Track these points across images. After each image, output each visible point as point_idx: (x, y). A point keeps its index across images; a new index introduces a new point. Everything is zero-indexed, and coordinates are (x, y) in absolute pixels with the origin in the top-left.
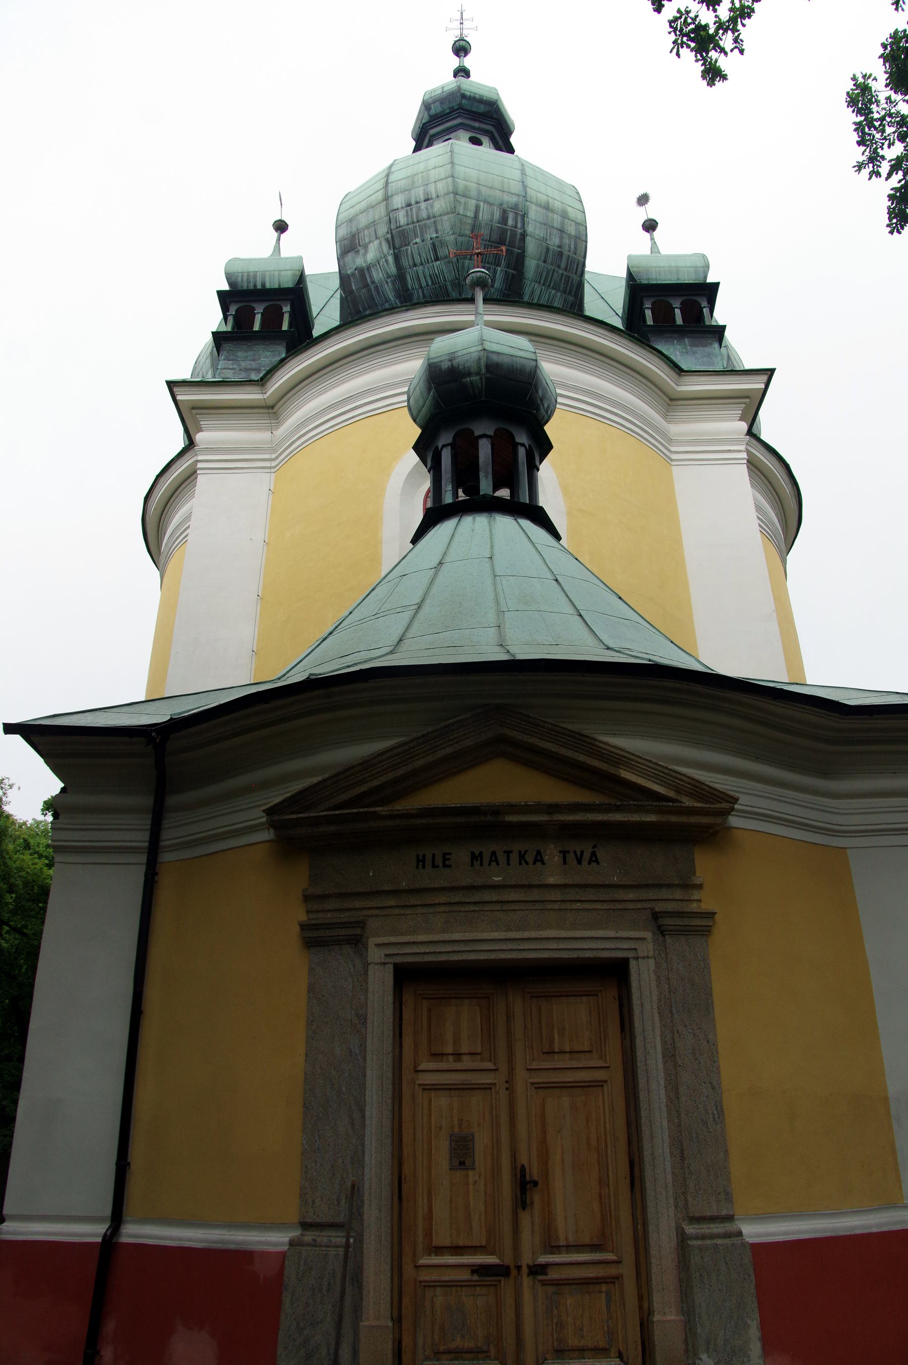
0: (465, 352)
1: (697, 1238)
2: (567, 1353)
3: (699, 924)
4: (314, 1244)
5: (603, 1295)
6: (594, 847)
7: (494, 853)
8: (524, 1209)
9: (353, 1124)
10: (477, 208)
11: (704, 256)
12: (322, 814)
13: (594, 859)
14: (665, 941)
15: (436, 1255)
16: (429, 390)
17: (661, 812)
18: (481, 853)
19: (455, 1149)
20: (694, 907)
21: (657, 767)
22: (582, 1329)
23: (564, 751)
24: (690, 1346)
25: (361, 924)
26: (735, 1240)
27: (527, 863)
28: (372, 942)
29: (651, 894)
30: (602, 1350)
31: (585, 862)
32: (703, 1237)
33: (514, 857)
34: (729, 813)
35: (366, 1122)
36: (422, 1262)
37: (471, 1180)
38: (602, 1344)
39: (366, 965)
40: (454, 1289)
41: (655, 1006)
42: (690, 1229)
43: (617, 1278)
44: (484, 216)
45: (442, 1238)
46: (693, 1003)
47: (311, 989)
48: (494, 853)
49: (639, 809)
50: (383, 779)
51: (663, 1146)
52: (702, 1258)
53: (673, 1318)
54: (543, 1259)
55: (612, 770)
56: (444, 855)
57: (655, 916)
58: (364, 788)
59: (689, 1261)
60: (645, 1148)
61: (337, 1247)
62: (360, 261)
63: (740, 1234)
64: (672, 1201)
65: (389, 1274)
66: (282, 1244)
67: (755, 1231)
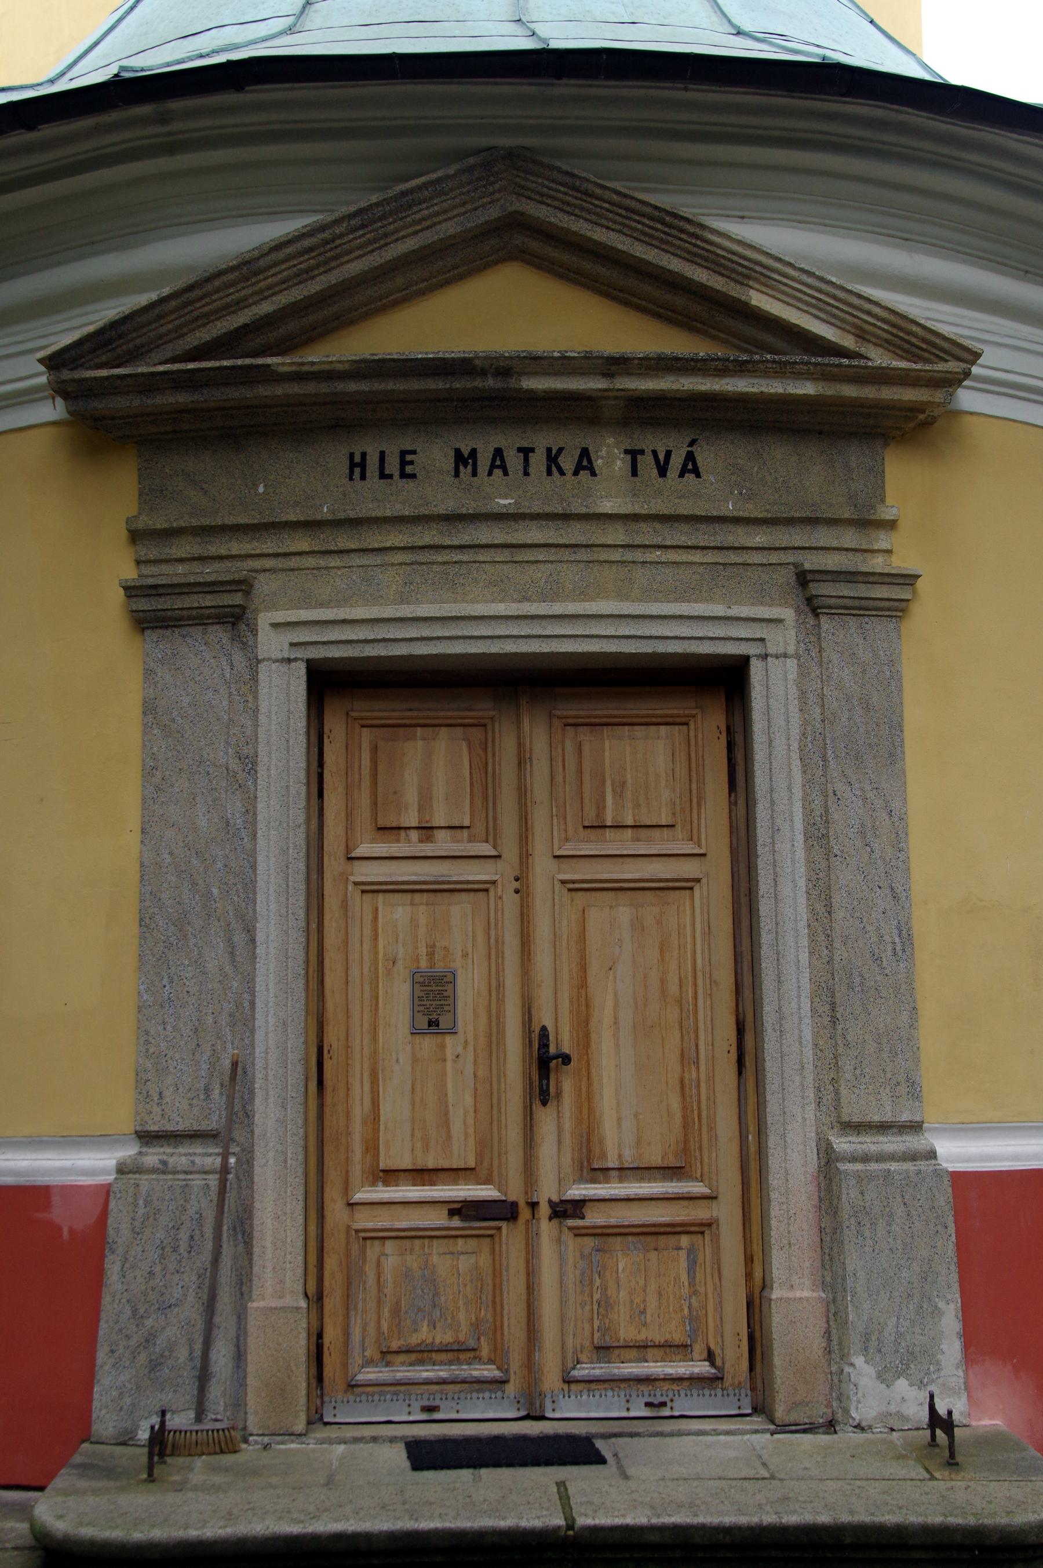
1: (854, 1159)
2: (617, 1352)
3: (885, 595)
4: (164, 1169)
5: (683, 1254)
6: (691, 444)
7: (498, 452)
8: (544, 1103)
9: (232, 954)
12: (161, 368)
13: (691, 467)
14: (819, 626)
15: (386, 1184)
17: (827, 376)
18: (473, 453)
19: (420, 998)
20: (877, 564)
21: (823, 286)
22: (643, 1312)
23: (640, 251)
24: (835, 1343)
25: (244, 586)
26: (922, 1165)
27: (562, 473)
28: (264, 619)
29: (798, 537)
30: (678, 1346)
31: (673, 472)
32: (866, 1158)
33: (538, 460)
34: (959, 383)
35: (258, 951)
36: (359, 1196)
37: (449, 1055)
38: (678, 1337)
40: (417, 1242)
41: (795, 746)
42: (842, 1144)
43: (709, 1225)
45: (397, 1154)
46: (867, 742)
47: (149, 708)
48: (498, 452)
49: (781, 370)
50: (283, 299)
51: (799, 997)
52: (862, 1193)
53: (806, 1294)
54: (577, 1191)
55: (735, 291)
56: (403, 453)
57: (803, 578)
59: (839, 1199)
60: (766, 1001)
61: (205, 1173)
63: (932, 1155)
64: (811, 1094)
65: (300, 1219)
66: (104, 1171)
67: (958, 1151)
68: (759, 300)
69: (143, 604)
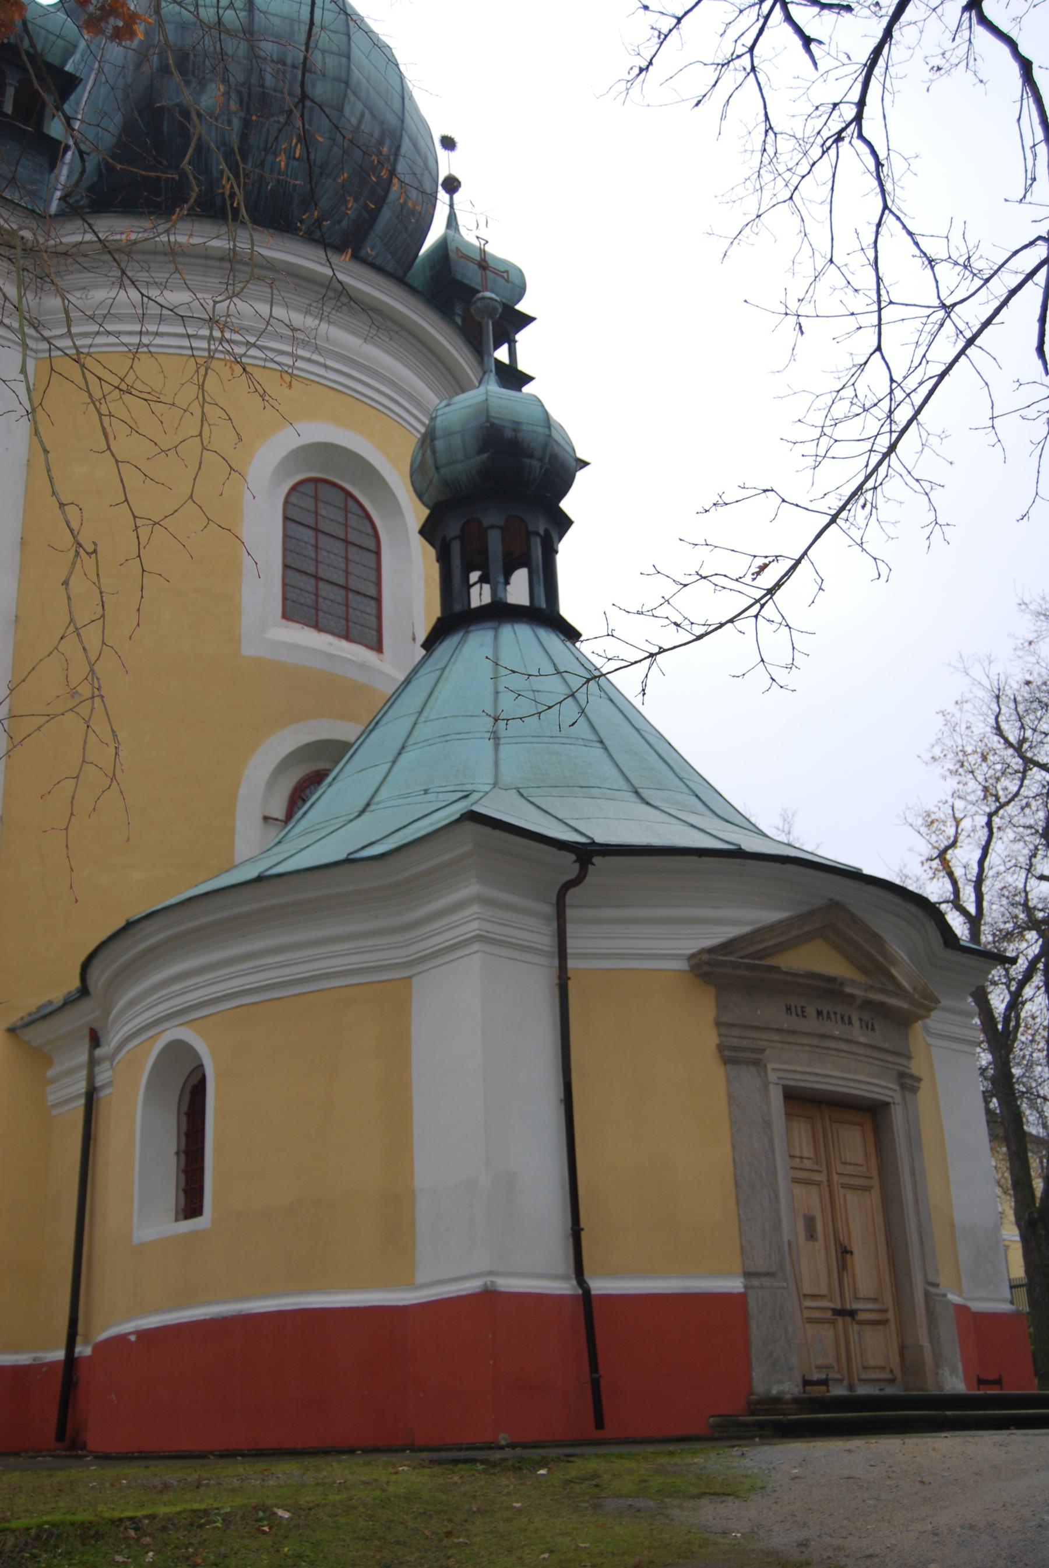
0: (530, 428)
10: (362, 115)
11: (521, 272)
12: (746, 961)
16: (481, 451)
33: (839, 1017)
39: (766, 1084)
47: (730, 1097)
48: (828, 1013)
54: (855, 1306)
56: (802, 1007)
58: (761, 946)
62: (187, 97)
68: (893, 971)
69: (727, 1053)
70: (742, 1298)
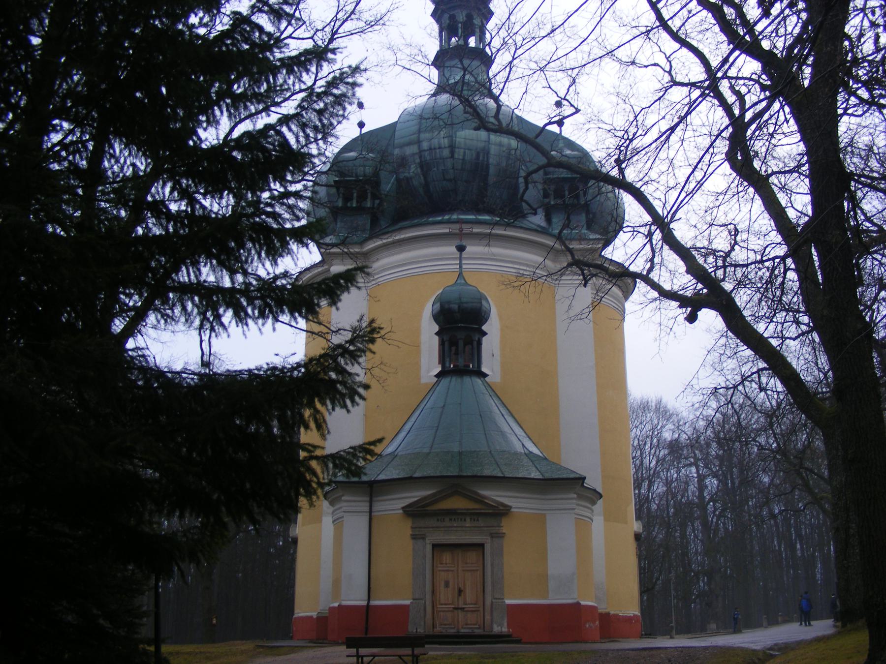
10: (465, 153)
44: (468, 158)
45: (442, 601)
57: (491, 534)
67: (508, 602)
70: (408, 606)
